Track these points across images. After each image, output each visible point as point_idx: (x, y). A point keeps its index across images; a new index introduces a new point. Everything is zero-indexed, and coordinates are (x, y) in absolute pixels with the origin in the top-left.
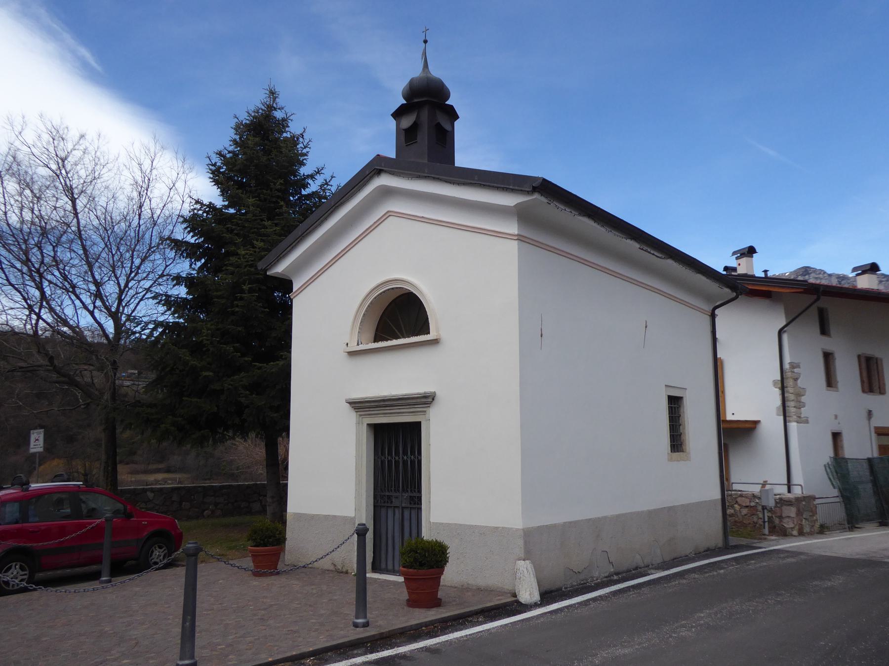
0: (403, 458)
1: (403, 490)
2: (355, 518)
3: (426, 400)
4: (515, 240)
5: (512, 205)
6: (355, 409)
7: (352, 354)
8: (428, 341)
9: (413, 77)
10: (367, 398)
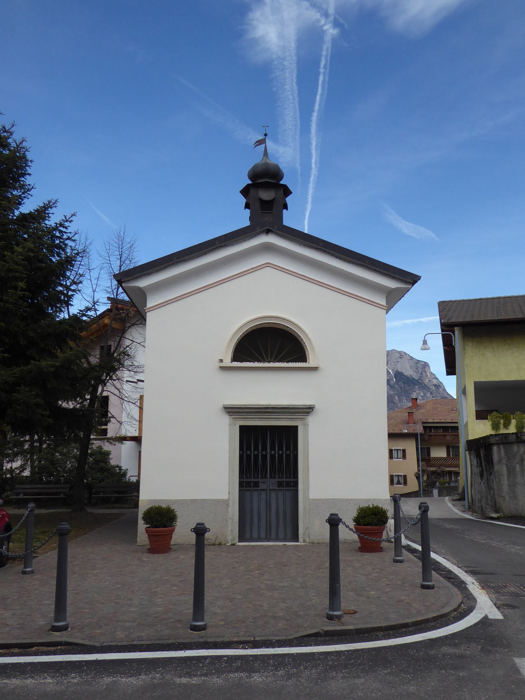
0: (270, 452)
1: (271, 478)
2: (228, 500)
3: (308, 410)
4: (384, 309)
5: (393, 287)
6: (228, 413)
7: (223, 368)
8: (295, 367)
9: (256, 163)
10: (248, 405)
